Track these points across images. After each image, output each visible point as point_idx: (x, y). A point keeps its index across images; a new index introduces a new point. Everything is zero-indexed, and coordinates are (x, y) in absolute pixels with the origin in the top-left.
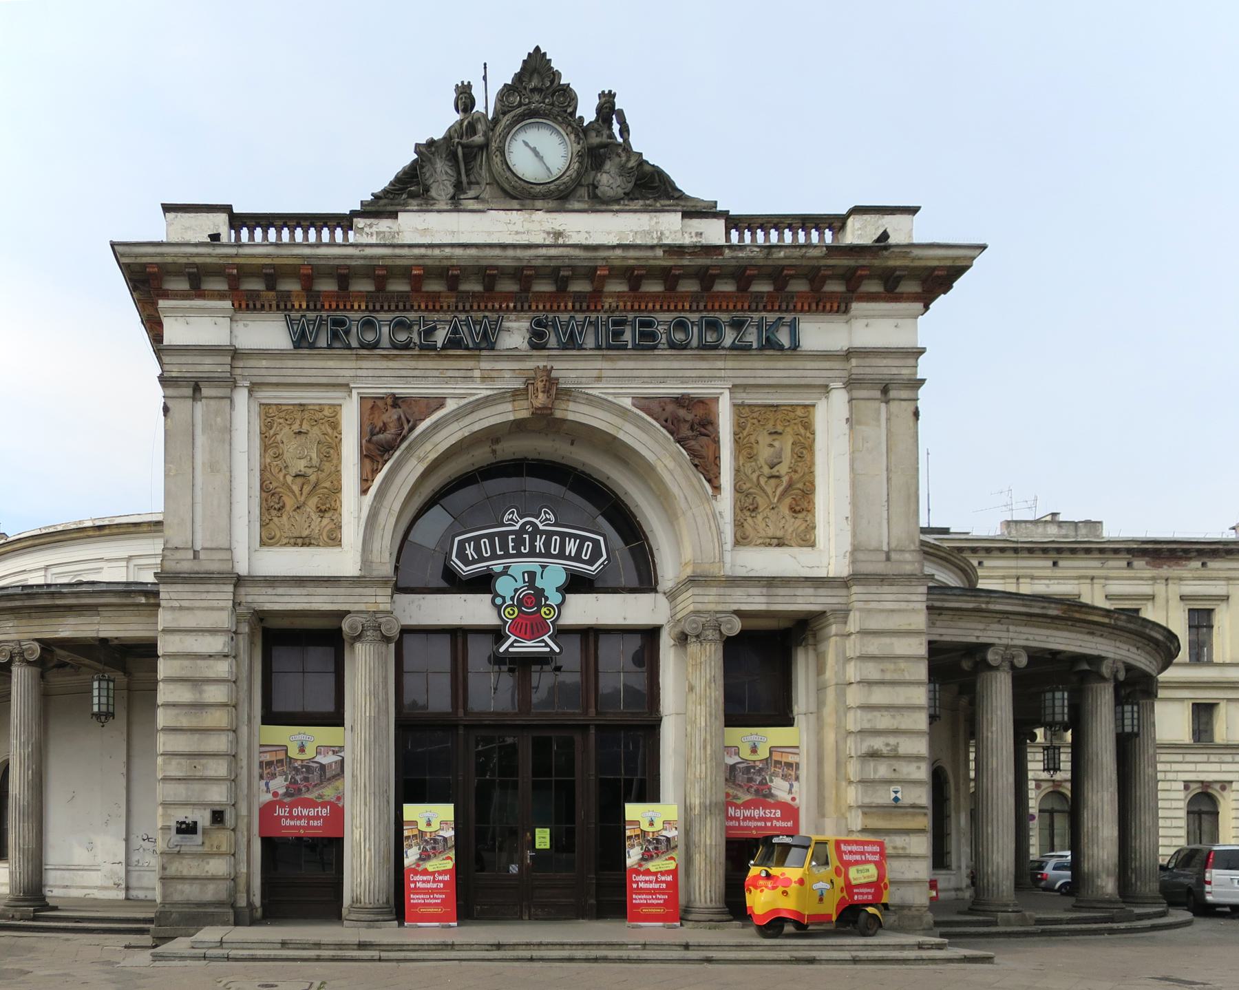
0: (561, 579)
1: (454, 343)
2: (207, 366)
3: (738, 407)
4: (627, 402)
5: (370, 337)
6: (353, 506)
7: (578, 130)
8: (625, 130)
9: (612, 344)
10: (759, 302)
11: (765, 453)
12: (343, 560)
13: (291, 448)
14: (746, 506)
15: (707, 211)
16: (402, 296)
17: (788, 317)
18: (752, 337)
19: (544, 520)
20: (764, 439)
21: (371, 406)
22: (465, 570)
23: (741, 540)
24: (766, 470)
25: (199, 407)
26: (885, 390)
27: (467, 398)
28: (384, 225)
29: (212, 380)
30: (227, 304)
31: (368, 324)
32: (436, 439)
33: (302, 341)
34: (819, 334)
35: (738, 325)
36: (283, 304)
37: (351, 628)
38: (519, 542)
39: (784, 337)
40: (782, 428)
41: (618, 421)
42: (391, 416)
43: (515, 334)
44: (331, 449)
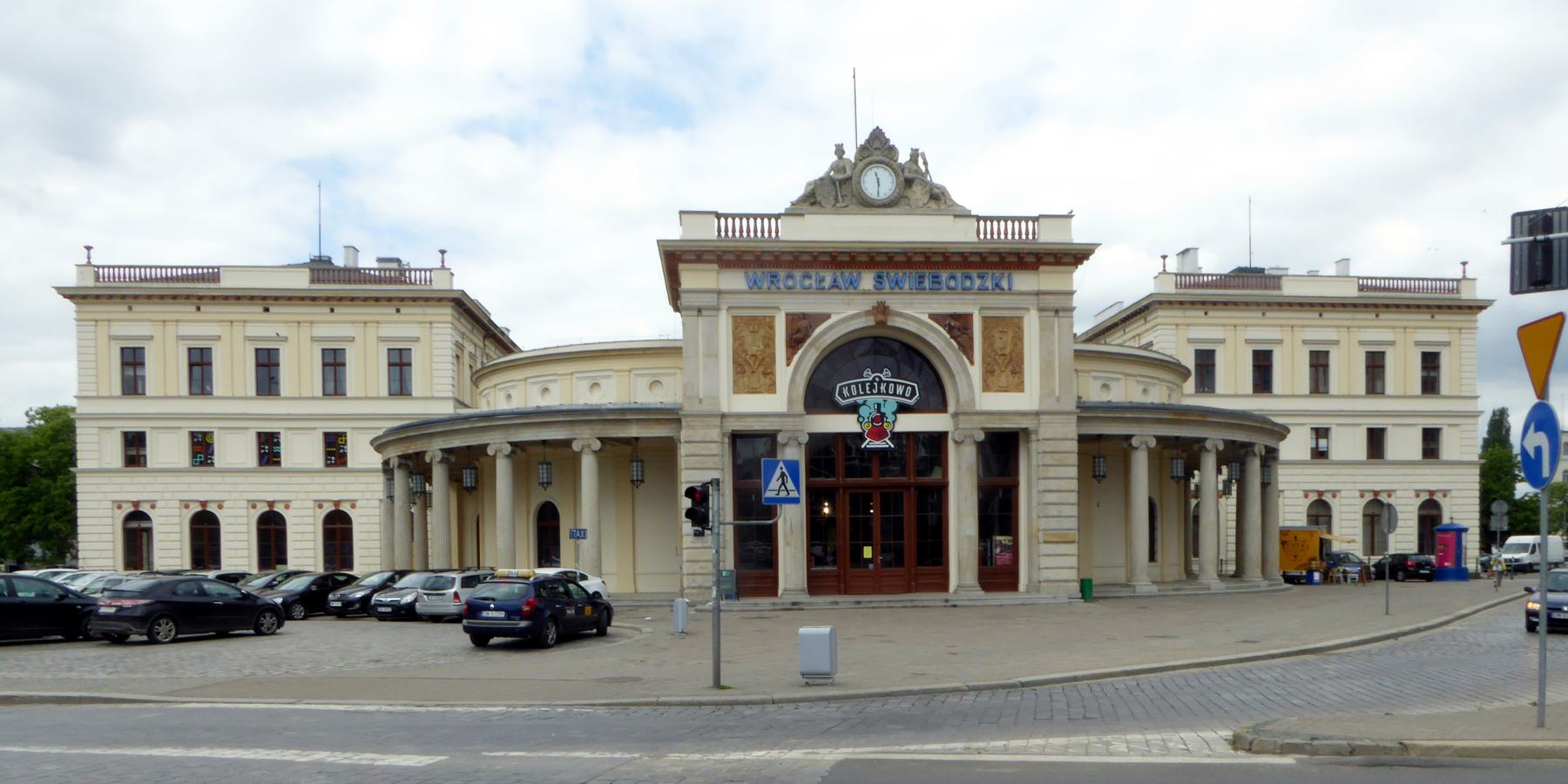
0: (895, 407)
1: (835, 285)
3: (985, 319)
4: (925, 318)
5: (790, 283)
7: (897, 169)
13: (748, 338)
14: (988, 372)
15: (964, 215)
18: (989, 284)
19: (886, 375)
20: (997, 335)
21: (792, 319)
22: (843, 402)
23: (986, 387)
25: (701, 319)
27: (844, 312)
31: (790, 276)
32: (824, 336)
34: (1024, 281)
35: (981, 277)
38: (872, 386)
39: (1005, 284)
40: (1006, 329)
42: (804, 323)
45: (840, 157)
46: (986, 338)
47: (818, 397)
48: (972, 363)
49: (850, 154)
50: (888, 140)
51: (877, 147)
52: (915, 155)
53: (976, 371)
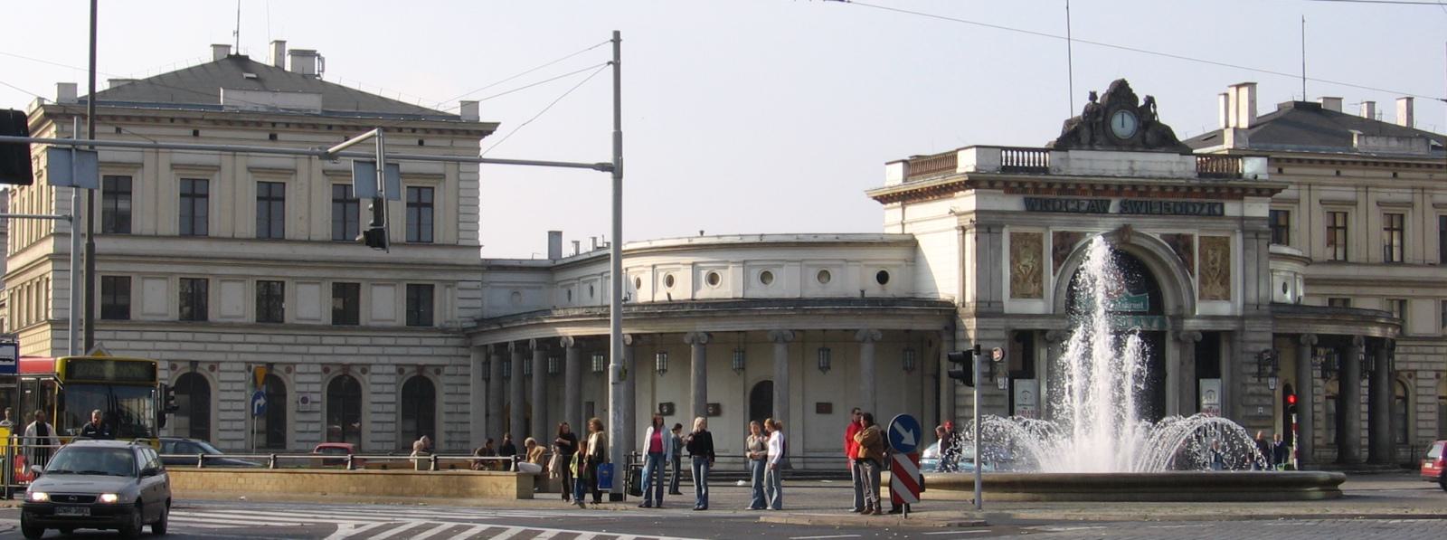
2: (993, 218)
3: (1200, 237)
4: (1157, 237)
8: (1155, 107)
10: (1208, 196)
11: (1211, 258)
14: (1203, 282)
16: (1072, 190)
17: (1219, 201)
18: (1205, 211)
20: (1210, 252)
24: (1211, 265)
26: (1257, 235)
29: (995, 226)
30: (1002, 191)
33: (1031, 206)
34: (1231, 209)
36: (1025, 191)
37: (1050, 337)
39: (1218, 210)
41: (1156, 246)
43: (1114, 206)
44: (1039, 253)
45: (1094, 102)
46: (1203, 256)
48: (1193, 275)
50: (1131, 90)
51: (1121, 92)
52: (1150, 100)
53: (1195, 282)
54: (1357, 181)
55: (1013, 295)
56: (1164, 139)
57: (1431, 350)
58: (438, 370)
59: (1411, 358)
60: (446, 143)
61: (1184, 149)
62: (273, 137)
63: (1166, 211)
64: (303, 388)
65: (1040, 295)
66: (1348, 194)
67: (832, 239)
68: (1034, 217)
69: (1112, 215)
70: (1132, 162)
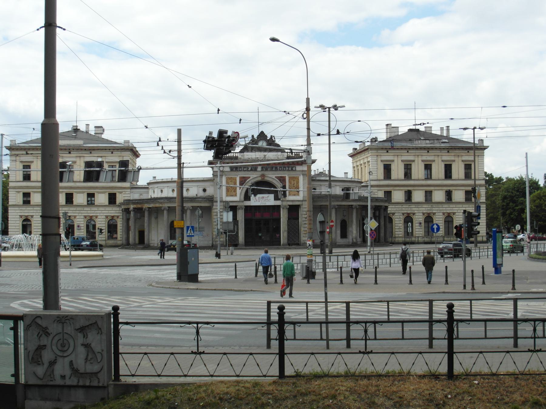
4: (274, 177)
6: (238, 191)
9: (272, 170)
12: (236, 199)
18: (290, 169)
27: (254, 177)
28: (242, 154)
34: (299, 168)
35: (289, 167)
42: (243, 179)
43: (259, 168)
46: (290, 182)
47: (247, 197)
49: (255, 137)
51: (262, 135)
54: (415, 154)
55: (227, 196)
56: (278, 149)
57: (441, 206)
58: (118, 217)
59: (434, 209)
60: (119, 153)
61: (282, 151)
62: (70, 153)
63: (276, 169)
64: (79, 223)
65: (236, 195)
66: (411, 158)
67: (189, 179)
68: (233, 173)
69: (259, 171)
70: (265, 155)
